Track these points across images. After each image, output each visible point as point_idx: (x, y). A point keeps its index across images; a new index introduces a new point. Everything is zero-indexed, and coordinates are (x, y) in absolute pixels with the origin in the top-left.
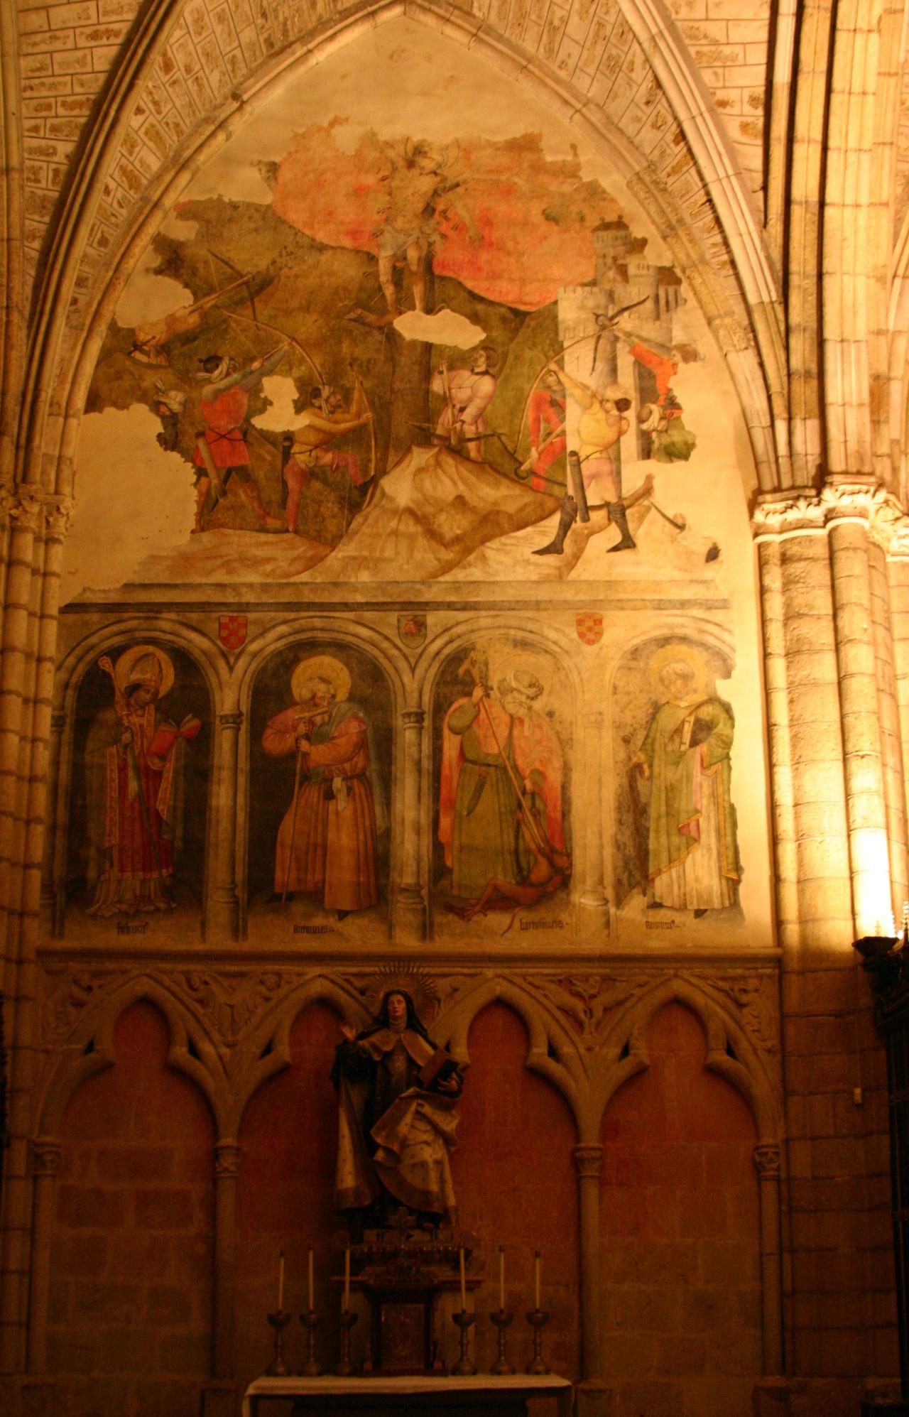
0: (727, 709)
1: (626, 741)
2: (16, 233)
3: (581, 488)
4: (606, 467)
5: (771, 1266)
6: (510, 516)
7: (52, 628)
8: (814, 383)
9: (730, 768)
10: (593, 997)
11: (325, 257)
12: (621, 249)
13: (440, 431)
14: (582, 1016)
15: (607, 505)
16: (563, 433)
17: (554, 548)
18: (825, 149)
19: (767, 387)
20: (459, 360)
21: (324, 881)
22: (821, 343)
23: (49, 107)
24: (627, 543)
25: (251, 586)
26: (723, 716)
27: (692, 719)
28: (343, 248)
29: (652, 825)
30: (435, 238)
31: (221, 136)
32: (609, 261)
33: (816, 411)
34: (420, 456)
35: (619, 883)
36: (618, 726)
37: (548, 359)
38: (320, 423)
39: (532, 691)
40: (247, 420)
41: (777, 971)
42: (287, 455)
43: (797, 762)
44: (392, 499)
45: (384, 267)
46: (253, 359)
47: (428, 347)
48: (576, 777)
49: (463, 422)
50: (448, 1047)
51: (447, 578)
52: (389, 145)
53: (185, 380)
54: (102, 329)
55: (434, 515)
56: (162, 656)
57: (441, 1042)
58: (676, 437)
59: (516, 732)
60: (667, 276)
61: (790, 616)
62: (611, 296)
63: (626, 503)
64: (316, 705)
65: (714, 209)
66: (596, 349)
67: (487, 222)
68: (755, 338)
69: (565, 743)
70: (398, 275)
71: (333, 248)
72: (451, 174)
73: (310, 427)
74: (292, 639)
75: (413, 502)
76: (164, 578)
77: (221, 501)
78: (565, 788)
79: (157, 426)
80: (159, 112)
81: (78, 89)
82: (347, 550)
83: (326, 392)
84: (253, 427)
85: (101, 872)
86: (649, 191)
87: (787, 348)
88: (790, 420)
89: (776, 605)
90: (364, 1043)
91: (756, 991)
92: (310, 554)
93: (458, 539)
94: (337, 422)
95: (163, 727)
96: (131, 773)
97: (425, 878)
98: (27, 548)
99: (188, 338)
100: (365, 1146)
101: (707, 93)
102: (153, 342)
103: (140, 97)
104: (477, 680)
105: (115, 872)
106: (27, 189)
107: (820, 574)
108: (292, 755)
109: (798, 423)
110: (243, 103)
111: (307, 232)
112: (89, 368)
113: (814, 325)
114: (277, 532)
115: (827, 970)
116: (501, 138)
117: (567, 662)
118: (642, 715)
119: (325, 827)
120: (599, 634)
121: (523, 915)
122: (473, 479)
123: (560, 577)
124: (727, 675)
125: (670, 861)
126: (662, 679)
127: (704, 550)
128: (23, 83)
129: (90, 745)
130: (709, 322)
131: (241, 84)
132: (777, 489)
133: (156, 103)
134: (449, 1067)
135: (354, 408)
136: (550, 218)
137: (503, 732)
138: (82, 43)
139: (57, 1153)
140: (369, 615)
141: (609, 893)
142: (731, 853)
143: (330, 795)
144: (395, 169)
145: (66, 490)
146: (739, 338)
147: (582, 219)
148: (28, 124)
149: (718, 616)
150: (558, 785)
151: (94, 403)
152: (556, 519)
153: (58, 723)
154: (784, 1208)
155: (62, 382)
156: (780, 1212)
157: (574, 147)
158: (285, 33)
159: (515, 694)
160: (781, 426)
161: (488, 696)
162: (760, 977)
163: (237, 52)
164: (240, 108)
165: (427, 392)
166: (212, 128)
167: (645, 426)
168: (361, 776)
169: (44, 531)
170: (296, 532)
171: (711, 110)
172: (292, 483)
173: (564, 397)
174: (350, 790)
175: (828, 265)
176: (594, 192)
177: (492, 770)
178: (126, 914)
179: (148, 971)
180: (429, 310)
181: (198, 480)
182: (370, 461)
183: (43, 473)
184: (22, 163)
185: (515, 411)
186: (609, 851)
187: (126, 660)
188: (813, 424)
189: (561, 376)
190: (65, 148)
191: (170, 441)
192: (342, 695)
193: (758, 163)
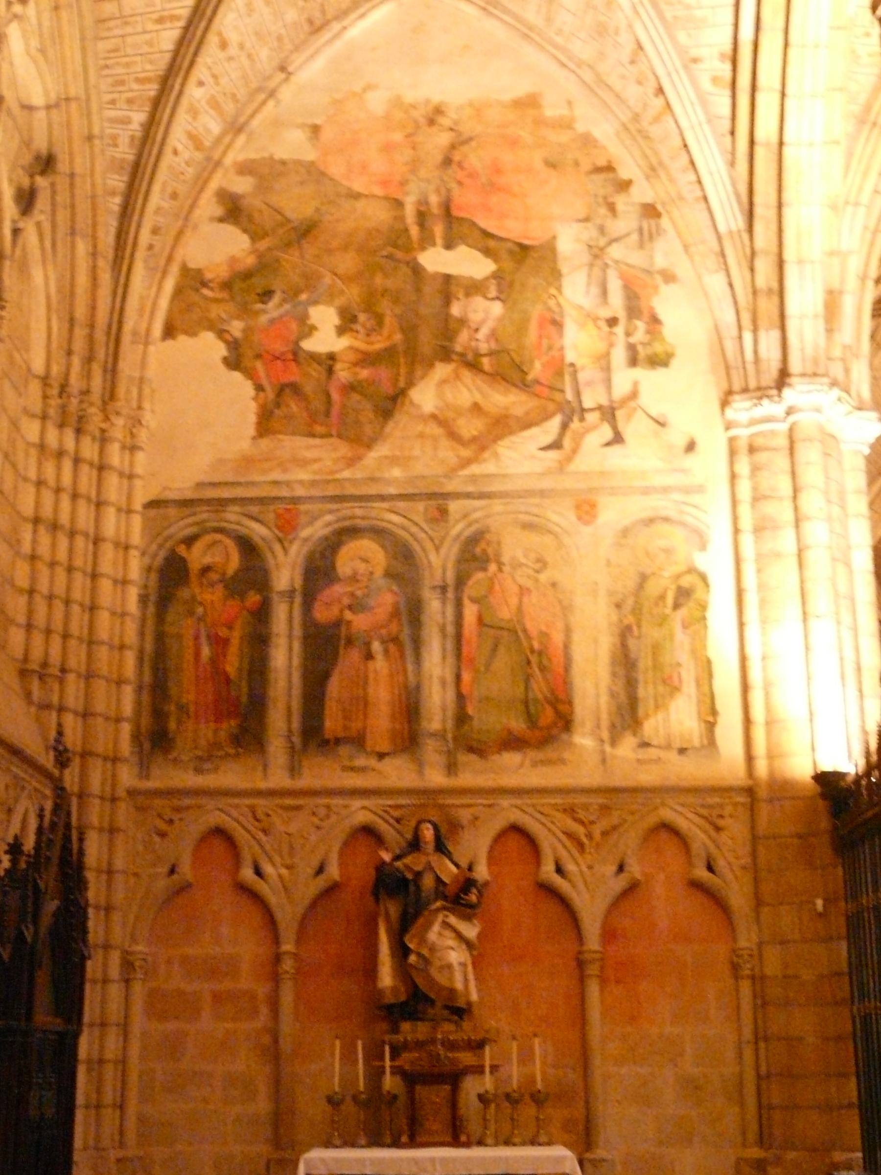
0: (703, 578)
1: (618, 606)
2: (99, 191)
3: (578, 394)
4: (599, 375)
5: (748, 1053)
6: (518, 419)
7: (137, 521)
8: (776, 299)
9: (706, 627)
10: (592, 823)
11: (360, 204)
12: (610, 189)
13: (458, 348)
14: (585, 840)
15: (600, 408)
16: (562, 349)
17: (556, 445)
18: (783, 95)
19: (736, 302)
20: (474, 288)
21: (365, 728)
22: (781, 264)
23: (122, 83)
24: (618, 438)
25: (301, 482)
26: (700, 584)
27: (673, 587)
28: (374, 196)
29: (641, 678)
30: (453, 185)
31: (271, 103)
32: (601, 200)
33: (777, 321)
34: (442, 370)
35: (613, 726)
36: (611, 593)
37: (549, 284)
38: (358, 344)
39: (538, 566)
40: (297, 343)
41: (749, 800)
42: (330, 371)
43: (764, 621)
44: (418, 407)
45: (410, 212)
46: (302, 291)
47: (448, 278)
48: (576, 637)
49: (477, 340)
50: (470, 869)
51: (466, 472)
52: (414, 107)
53: (245, 311)
54: (175, 269)
55: (454, 420)
56: (229, 543)
57: (464, 864)
58: (658, 348)
59: (525, 600)
60: (650, 211)
61: (757, 498)
62: (602, 230)
63: (615, 405)
64: (357, 581)
65: (688, 152)
66: (589, 276)
67: (498, 170)
68: (725, 263)
69: (566, 609)
70: (422, 217)
71: (366, 196)
72: (468, 128)
73: (351, 348)
74: (336, 526)
75: (437, 408)
76: (230, 478)
77: (276, 411)
78: (567, 647)
79: (221, 350)
80: (217, 84)
81: (148, 67)
82: (381, 451)
83: (362, 317)
84: (300, 348)
85: (180, 722)
86: (634, 139)
87: (752, 270)
88: (755, 330)
89: (744, 489)
90: (398, 864)
91: (731, 816)
92: (350, 454)
93: (474, 439)
94: (372, 343)
95: (230, 602)
96: (203, 640)
97: (450, 724)
98: (115, 456)
99: (247, 275)
100: (401, 951)
101: (682, 51)
102: (217, 280)
103: (200, 71)
104: (492, 556)
105: (190, 725)
106: (108, 153)
107: (782, 462)
108: (338, 623)
109: (762, 335)
110: (290, 74)
111: (345, 183)
112: (164, 303)
113: (774, 249)
114: (322, 436)
115: (793, 798)
116: (508, 96)
117: (566, 540)
118: (631, 584)
119: (366, 682)
120: (594, 516)
121: (532, 754)
122: (486, 388)
123: (561, 467)
124: (703, 547)
125: (657, 707)
126: (647, 554)
127: (682, 443)
128: (102, 62)
129: (170, 617)
130: (686, 248)
131: (287, 57)
132: (745, 390)
133: (215, 77)
134: (468, 884)
135: (385, 332)
136: (551, 165)
137: (514, 601)
138: (150, 26)
139: (144, 960)
140: (401, 505)
141: (605, 735)
142: (708, 701)
143: (369, 656)
144: (417, 126)
145: (147, 405)
146: (712, 262)
147: (577, 164)
148: (108, 97)
149: (696, 499)
150: (561, 645)
151: (169, 332)
152: (556, 422)
153: (143, 600)
154: (759, 1002)
155: (141, 315)
156: (755, 1005)
157: (569, 103)
158: (323, 12)
159: (524, 569)
160: (748, 337)
161: (500, 570)
162: (736, 805)
163: (283, 31)
164: (287, 80)
165: (447, 317)
166: (262, 96)
167: (632, 340)
168: (395, 640)
169: (128, 439)
170: (339, 436)
171: (686, 67)
172: (335, 396)
173: (562, 317)
174: (386, 651)
175: (787, 196)
176: (587, 141)
177: (505, 633)
178: (200, 758)
179: (220, 807)
180: (449, 245)
181: (257, 394)
182: (398, 374)
183: (128, 391)
184: (102, 130)
185: (522, 328)
186: (604, 699)
187: (198, 547)
188: (776, 334)
189: (561, 300)
190: (139, 117)
191: (234, 362)
192: (379, 572)
193: (726, 111)
